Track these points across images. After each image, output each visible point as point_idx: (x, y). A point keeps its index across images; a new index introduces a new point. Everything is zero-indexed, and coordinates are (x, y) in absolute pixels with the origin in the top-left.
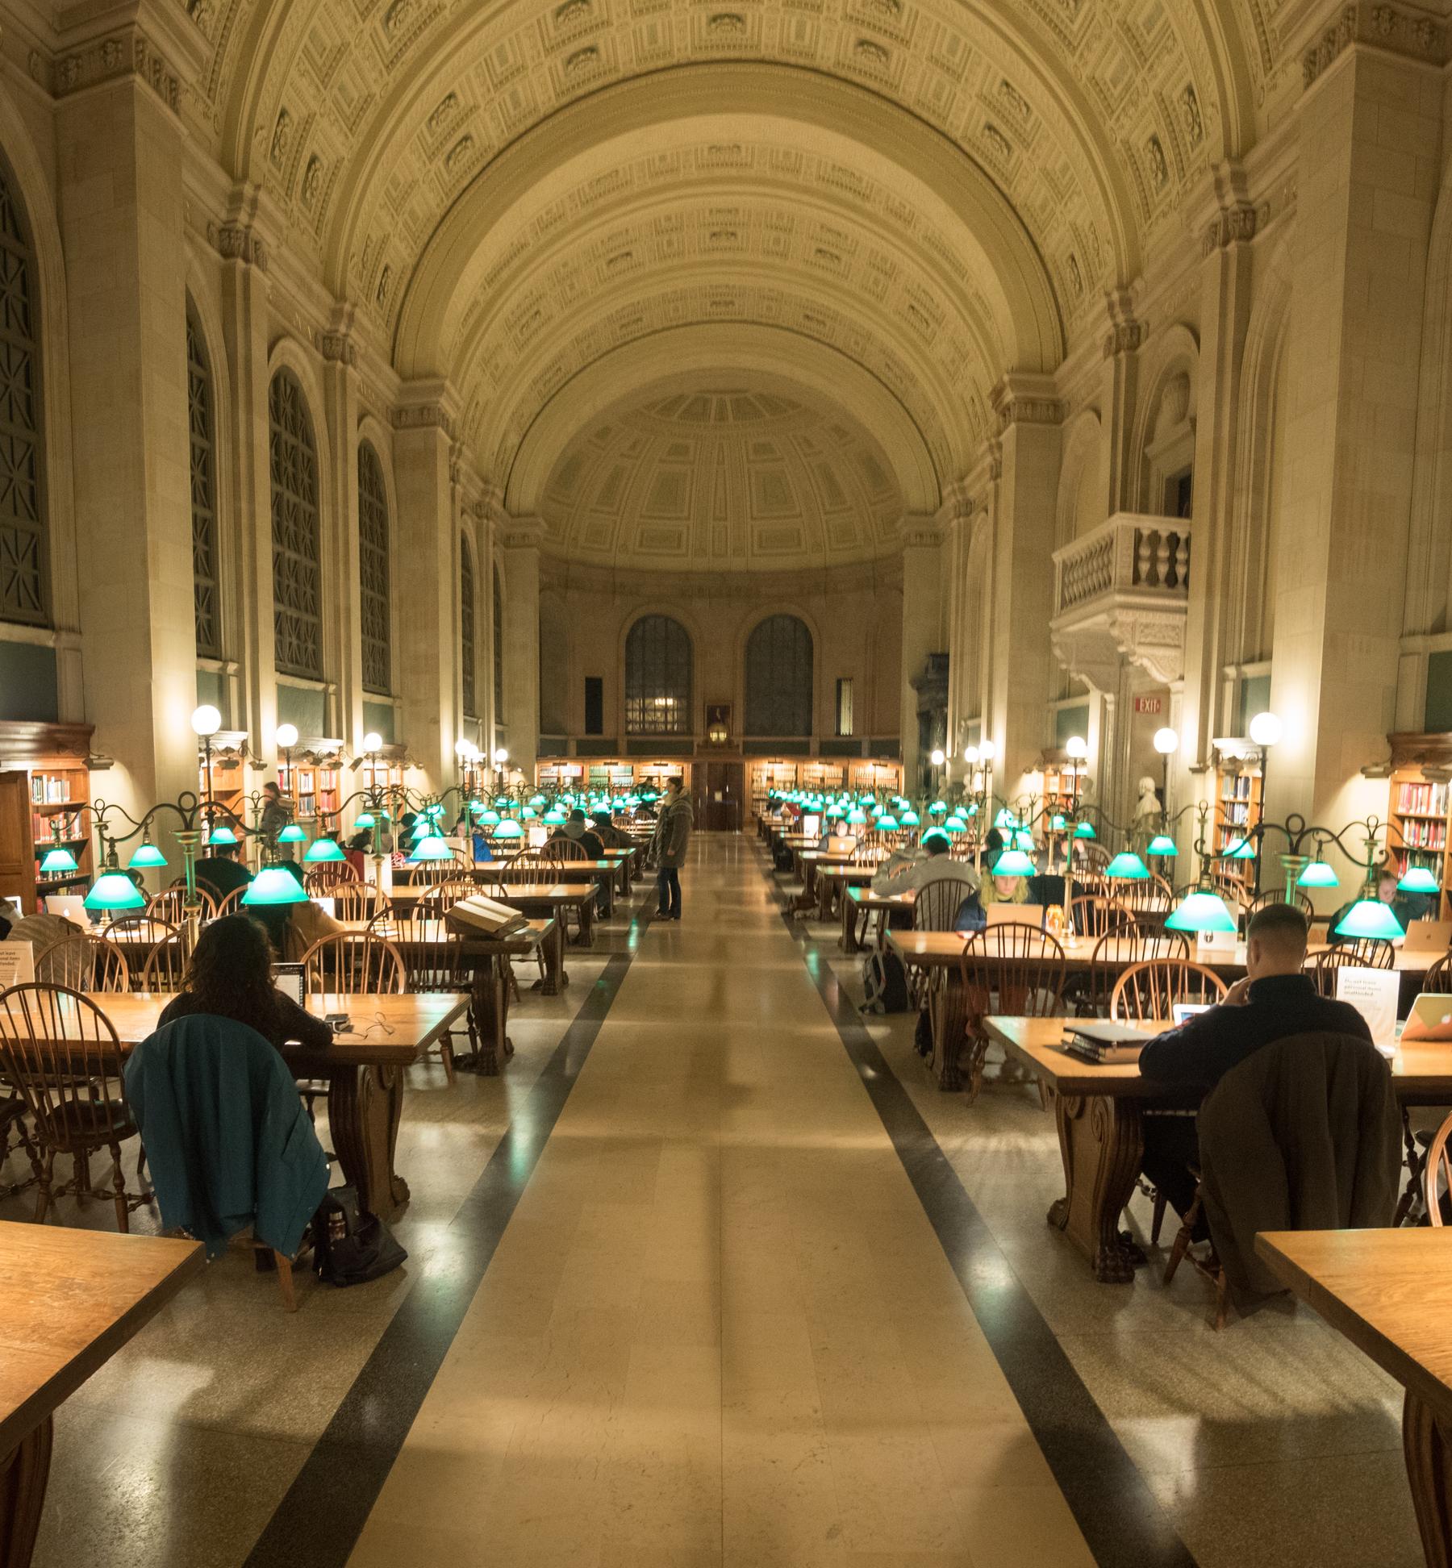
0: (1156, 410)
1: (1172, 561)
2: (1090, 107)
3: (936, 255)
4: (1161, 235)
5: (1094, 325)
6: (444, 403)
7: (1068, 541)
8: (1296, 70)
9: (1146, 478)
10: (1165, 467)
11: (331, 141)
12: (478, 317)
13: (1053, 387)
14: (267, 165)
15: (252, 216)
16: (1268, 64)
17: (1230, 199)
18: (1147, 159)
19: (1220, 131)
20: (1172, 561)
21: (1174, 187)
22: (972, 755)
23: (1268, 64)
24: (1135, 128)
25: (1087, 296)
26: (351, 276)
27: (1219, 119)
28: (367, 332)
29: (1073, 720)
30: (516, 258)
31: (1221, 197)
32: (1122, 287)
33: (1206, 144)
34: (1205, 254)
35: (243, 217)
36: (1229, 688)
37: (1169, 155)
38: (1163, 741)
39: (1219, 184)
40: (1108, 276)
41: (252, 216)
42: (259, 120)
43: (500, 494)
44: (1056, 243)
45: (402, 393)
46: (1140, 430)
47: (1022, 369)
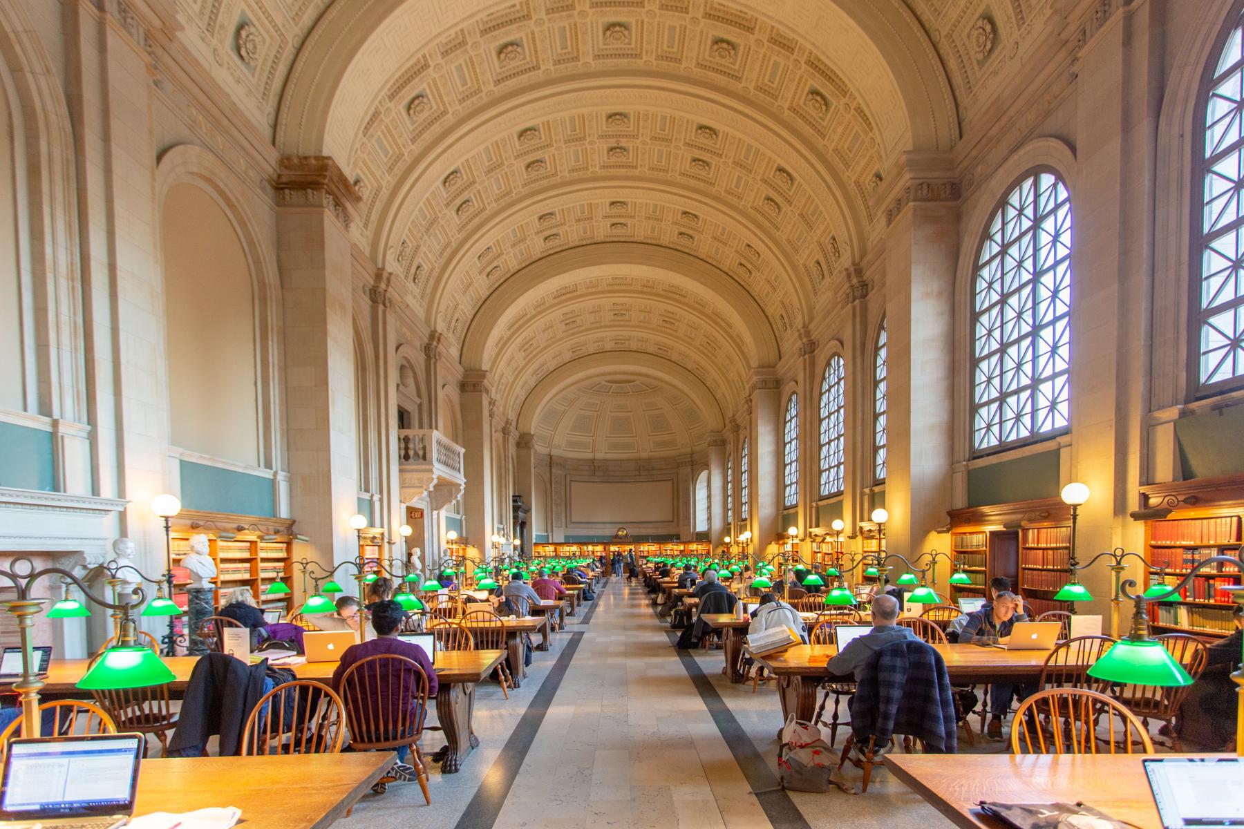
4: (825, 298)
5: (791, 343)
8: (883, 221)
11: (429, 259)
14: (396, 264)
15: (387, 286)
16: (871, 219)
17: (855, 281)
18: (814, 271)
19: (849, 253)
21: (828, 280)
23: (871, 219)
24: (808, 255)
25: (789, 331)
26: (439, 320)
27: (849, 248)
31: (850, 281)
32: (804, 326)
33: (842, 259)
34: (843, 308)
35: (383, 286)
39: (849, 276)
40: (799, 322)
41: (387, 286)
42: (390, 243)
43: (514, 424)
44: (773, 309)
45: (465, 376)
47: (760, 366)
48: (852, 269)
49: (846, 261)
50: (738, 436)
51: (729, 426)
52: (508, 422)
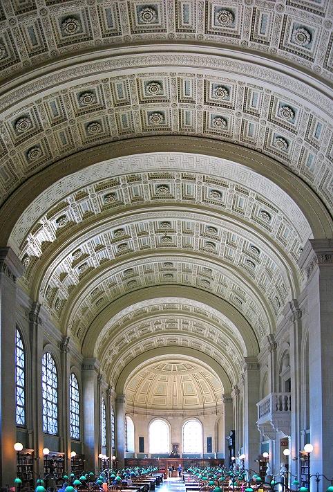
0: (282, 364)
1: (286, 404)
2: (259, 290)
3: (225, 329)
4: (280, 319)
5: (264, 344)
6: (95, 364)
7: (263, 398)
9: (280, 382)
10: (285, 379)
12: (106, 343)
13: (257, 360)
18: (275, 301)
20: (286, 404)
22: (241, 457)
28: (74, 344)
29: (265, 449)
30: (116, 330)
36: (303, 437)
37: (280, 300)
38: (286, 452)
39: (291, 306)
43: (113, 388)
46: (278, 368)
48: (293, 303)
49: (289, 298)
50: (239, 396)
51: (234, 391)
52: (110, 387)
